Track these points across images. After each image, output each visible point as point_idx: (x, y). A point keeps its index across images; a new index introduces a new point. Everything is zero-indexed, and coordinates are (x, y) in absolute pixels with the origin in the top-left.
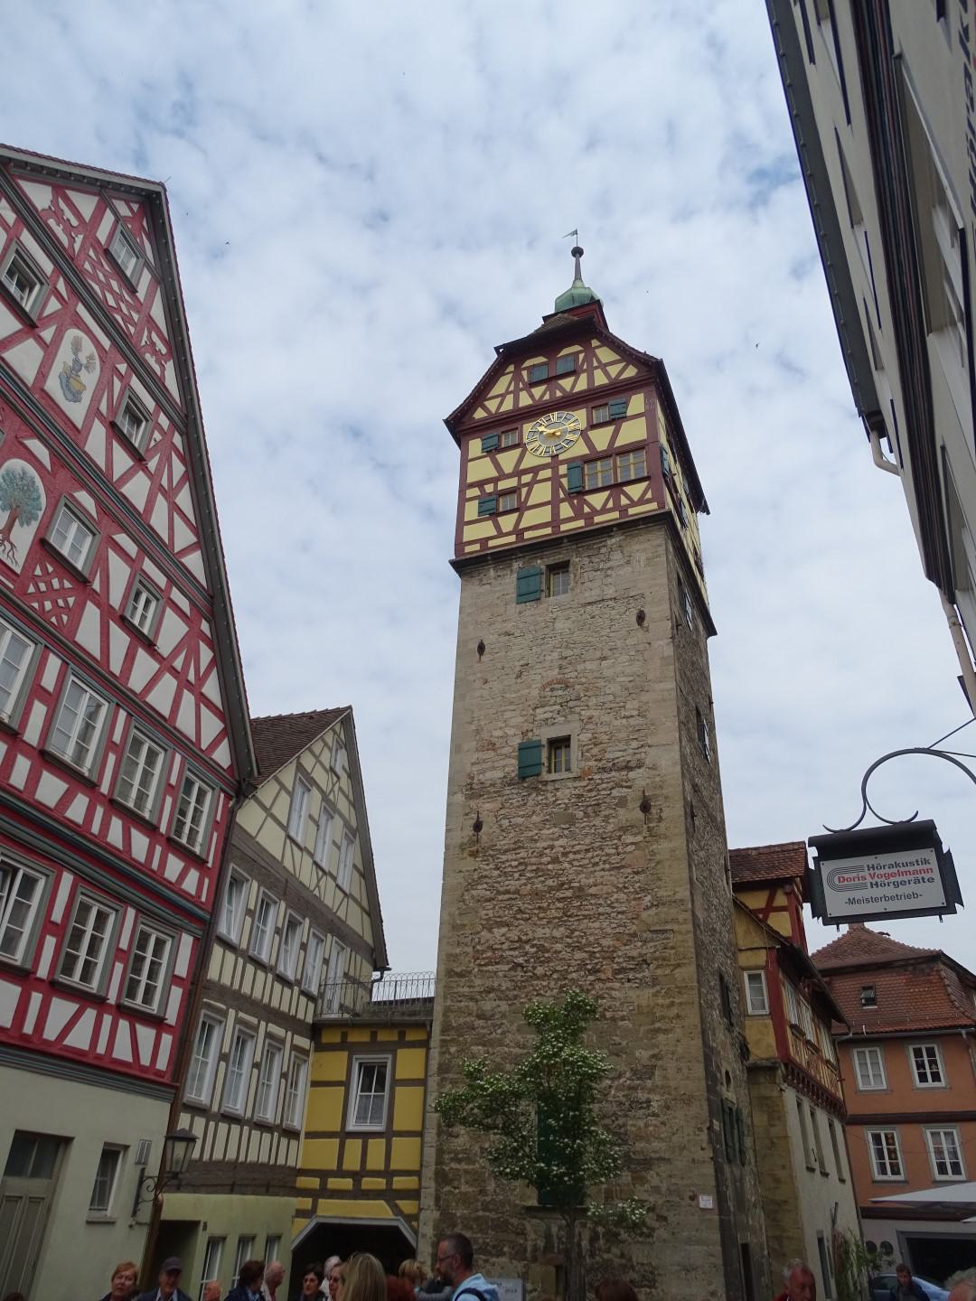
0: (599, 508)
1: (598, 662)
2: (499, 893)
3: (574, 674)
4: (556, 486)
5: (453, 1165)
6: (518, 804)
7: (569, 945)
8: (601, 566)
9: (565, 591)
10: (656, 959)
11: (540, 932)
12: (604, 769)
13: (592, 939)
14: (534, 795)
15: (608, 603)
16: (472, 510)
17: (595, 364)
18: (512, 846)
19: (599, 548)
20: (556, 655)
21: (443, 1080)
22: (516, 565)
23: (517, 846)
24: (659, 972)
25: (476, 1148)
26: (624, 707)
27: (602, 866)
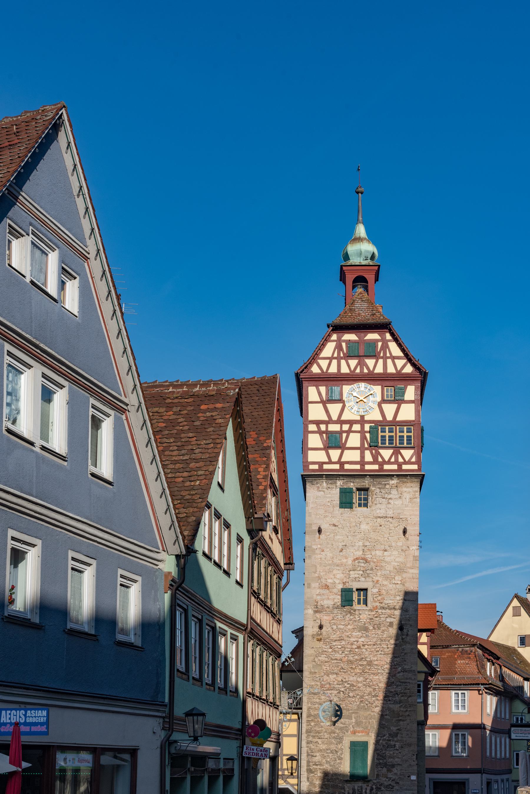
0: (387, 460)
1: (382, 552)
2: (332, 659)
3: (370, 556)
4: (363, 438)
5: (314, 767)
6: (340, 619)
7: (364, 685)
8: (386, 496)
9: (366, 505)
10: (402, 693)
11: (351, 679)
12: (383, 608)
13: (375, 683)
14: (349, 615)
15: (388, 519)
17: (388, 355)
18: (338, 639)
19: (385, 484)
20: (361, 543)
21: (308, 735)
22: (339, 483)
23: (341, 639)
24: (402, 698)
25: (324, 761)
26: (394, 578)
27: (380, 652)
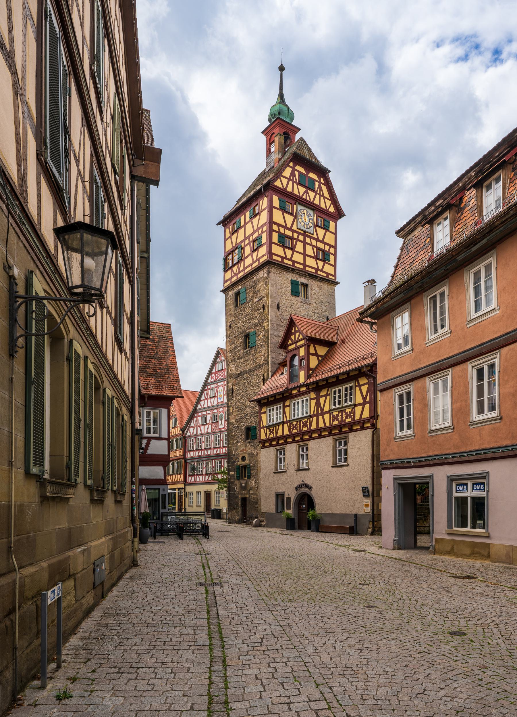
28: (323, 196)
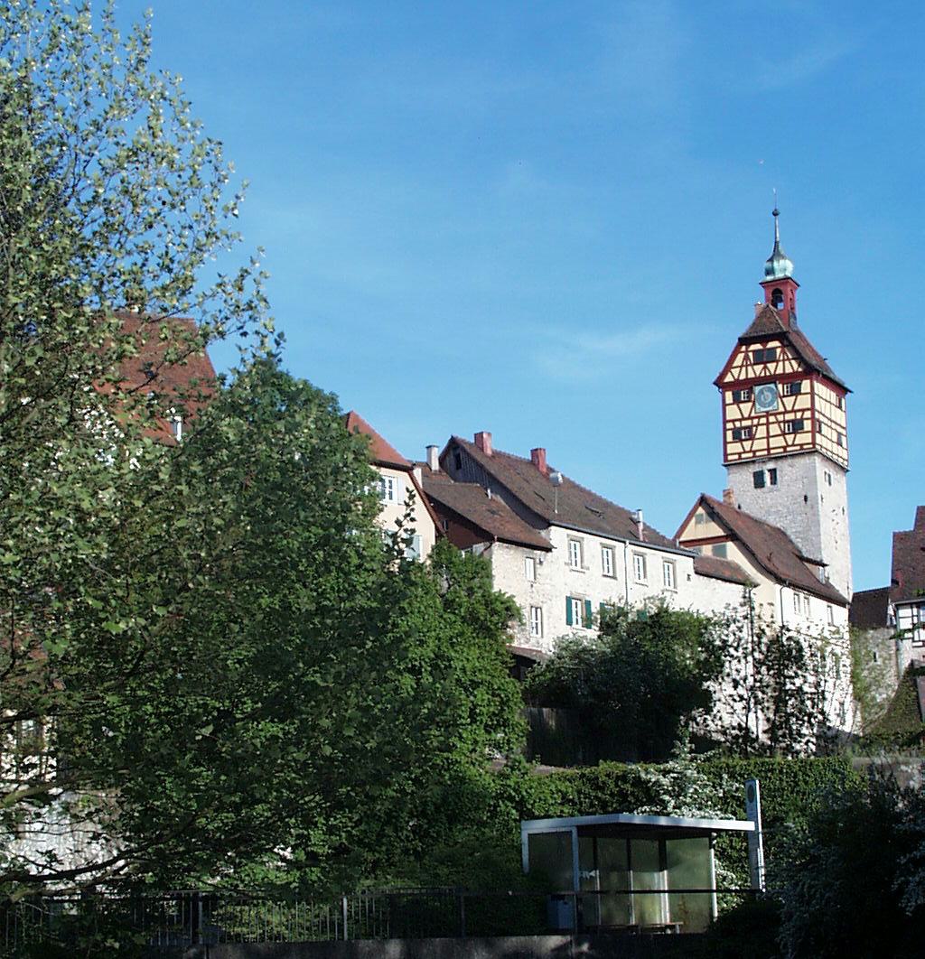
16: (729, 434)
28: (788, 359)
